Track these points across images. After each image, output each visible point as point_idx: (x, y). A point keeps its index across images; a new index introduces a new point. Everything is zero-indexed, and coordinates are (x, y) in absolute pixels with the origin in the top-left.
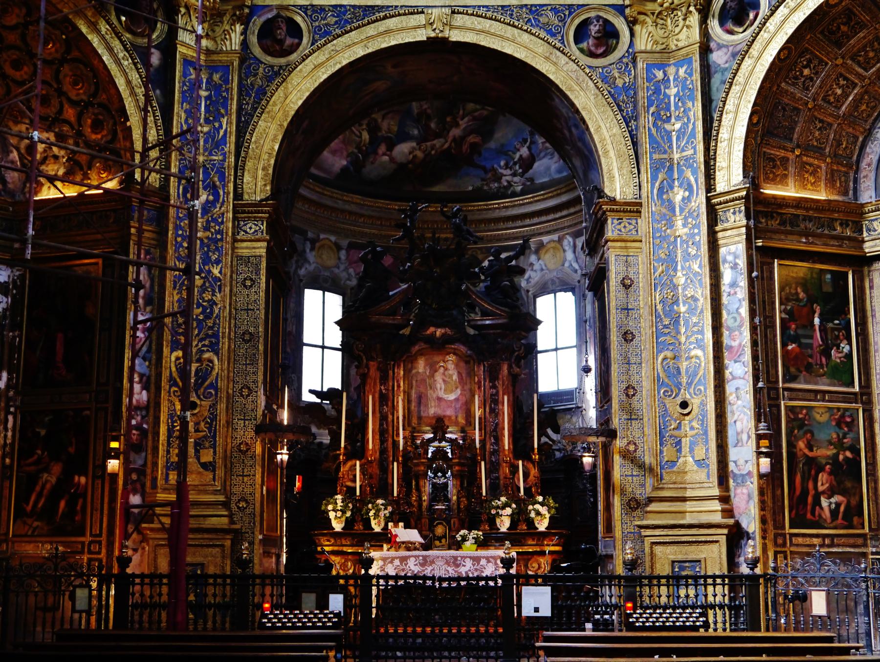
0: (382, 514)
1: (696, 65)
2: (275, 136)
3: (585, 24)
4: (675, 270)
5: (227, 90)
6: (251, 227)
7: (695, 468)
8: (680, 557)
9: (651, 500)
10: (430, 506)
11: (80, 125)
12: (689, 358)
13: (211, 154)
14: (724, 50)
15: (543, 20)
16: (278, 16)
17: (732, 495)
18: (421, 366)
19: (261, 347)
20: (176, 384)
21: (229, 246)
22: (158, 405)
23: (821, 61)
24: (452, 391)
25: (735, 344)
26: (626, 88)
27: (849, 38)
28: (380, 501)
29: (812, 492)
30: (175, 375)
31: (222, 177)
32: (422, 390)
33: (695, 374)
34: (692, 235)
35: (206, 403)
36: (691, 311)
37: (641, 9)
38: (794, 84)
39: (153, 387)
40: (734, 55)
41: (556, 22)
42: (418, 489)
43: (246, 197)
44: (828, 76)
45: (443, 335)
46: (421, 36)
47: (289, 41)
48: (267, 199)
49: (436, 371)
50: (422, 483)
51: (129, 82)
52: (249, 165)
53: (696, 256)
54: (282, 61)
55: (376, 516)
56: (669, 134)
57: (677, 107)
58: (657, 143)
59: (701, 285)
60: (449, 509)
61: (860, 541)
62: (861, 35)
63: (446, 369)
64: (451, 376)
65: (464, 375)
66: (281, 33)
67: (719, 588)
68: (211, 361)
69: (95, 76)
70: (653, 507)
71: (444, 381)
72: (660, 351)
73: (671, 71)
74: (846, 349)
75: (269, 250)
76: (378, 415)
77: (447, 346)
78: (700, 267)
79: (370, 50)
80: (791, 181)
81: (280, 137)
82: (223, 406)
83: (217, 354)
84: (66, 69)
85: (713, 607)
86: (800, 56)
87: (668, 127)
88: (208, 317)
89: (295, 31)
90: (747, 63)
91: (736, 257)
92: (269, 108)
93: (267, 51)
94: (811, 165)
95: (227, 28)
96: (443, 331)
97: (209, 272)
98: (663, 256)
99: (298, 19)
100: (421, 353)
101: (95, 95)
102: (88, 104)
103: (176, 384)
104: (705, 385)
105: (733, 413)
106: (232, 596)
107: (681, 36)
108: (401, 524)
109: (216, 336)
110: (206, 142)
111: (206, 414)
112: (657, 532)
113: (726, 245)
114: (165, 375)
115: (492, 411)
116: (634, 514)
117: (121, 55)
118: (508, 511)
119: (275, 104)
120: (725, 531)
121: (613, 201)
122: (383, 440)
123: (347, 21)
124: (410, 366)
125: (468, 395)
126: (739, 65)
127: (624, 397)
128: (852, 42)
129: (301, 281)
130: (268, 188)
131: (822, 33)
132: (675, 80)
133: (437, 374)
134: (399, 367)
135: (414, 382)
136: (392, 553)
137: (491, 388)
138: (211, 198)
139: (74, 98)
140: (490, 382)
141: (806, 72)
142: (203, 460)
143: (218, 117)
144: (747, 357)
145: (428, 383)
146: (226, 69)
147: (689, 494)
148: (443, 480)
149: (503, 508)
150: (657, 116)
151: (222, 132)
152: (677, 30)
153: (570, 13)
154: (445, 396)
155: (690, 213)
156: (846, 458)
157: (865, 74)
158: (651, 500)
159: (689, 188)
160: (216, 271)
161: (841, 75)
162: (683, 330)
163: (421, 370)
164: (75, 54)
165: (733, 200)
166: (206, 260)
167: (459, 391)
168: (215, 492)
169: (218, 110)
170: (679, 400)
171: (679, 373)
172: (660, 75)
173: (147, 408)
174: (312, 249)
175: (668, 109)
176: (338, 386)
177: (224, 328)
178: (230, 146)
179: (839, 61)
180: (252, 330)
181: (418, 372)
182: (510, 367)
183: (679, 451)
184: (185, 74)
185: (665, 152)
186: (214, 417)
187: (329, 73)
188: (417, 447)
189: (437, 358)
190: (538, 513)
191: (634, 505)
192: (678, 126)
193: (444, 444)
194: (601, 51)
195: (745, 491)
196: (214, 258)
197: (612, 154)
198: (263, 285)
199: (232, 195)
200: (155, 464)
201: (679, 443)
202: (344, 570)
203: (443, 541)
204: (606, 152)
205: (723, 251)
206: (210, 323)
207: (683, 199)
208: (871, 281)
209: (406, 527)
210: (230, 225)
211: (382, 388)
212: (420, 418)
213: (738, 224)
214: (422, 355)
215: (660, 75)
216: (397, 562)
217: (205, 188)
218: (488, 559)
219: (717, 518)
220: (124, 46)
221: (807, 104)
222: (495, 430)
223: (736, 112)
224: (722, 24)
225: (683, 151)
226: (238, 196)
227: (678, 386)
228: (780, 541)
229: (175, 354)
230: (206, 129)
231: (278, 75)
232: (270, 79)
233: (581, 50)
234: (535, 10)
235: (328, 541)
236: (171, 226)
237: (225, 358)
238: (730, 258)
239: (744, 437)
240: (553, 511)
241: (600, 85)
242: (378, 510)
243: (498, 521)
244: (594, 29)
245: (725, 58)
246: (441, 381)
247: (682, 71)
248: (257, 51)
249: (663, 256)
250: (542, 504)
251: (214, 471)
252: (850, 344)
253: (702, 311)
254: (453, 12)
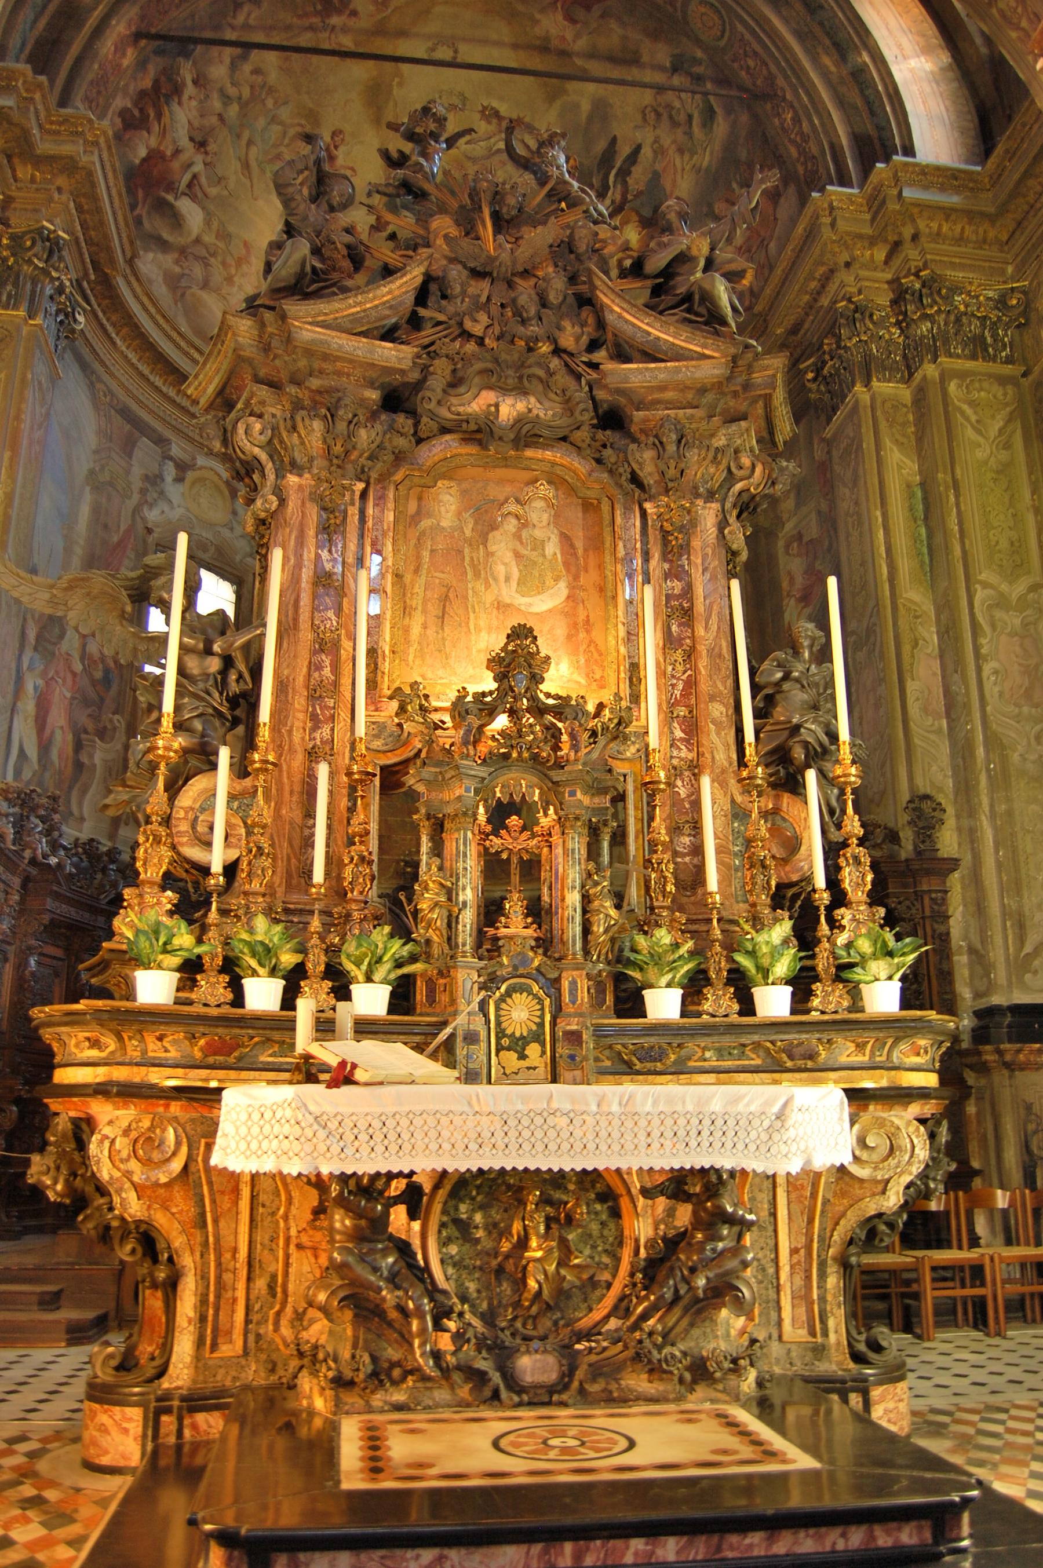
24: (541, 589)
45: (520, 421)
49: (494, 527)
63: (524, 524)
64: (539, 545)
65: (579, 545)
71: (517, 555)
77: (529, 453)
96: (521, 406)
100: (447, 471)
124: (412, 507)
129: (149, 531)
133: (495, 536)
134: (381, 498)
135: (426, 554)
137: (667, 576)
140: (664, 557)
163: (447, 521)
174: (180, 480)
181: (437, 528)
189: (496, 492)
202: (147, 1162)
203: (533, 1050)
211: (325, 554)
235: (95, 1044)
246: (509, 556)
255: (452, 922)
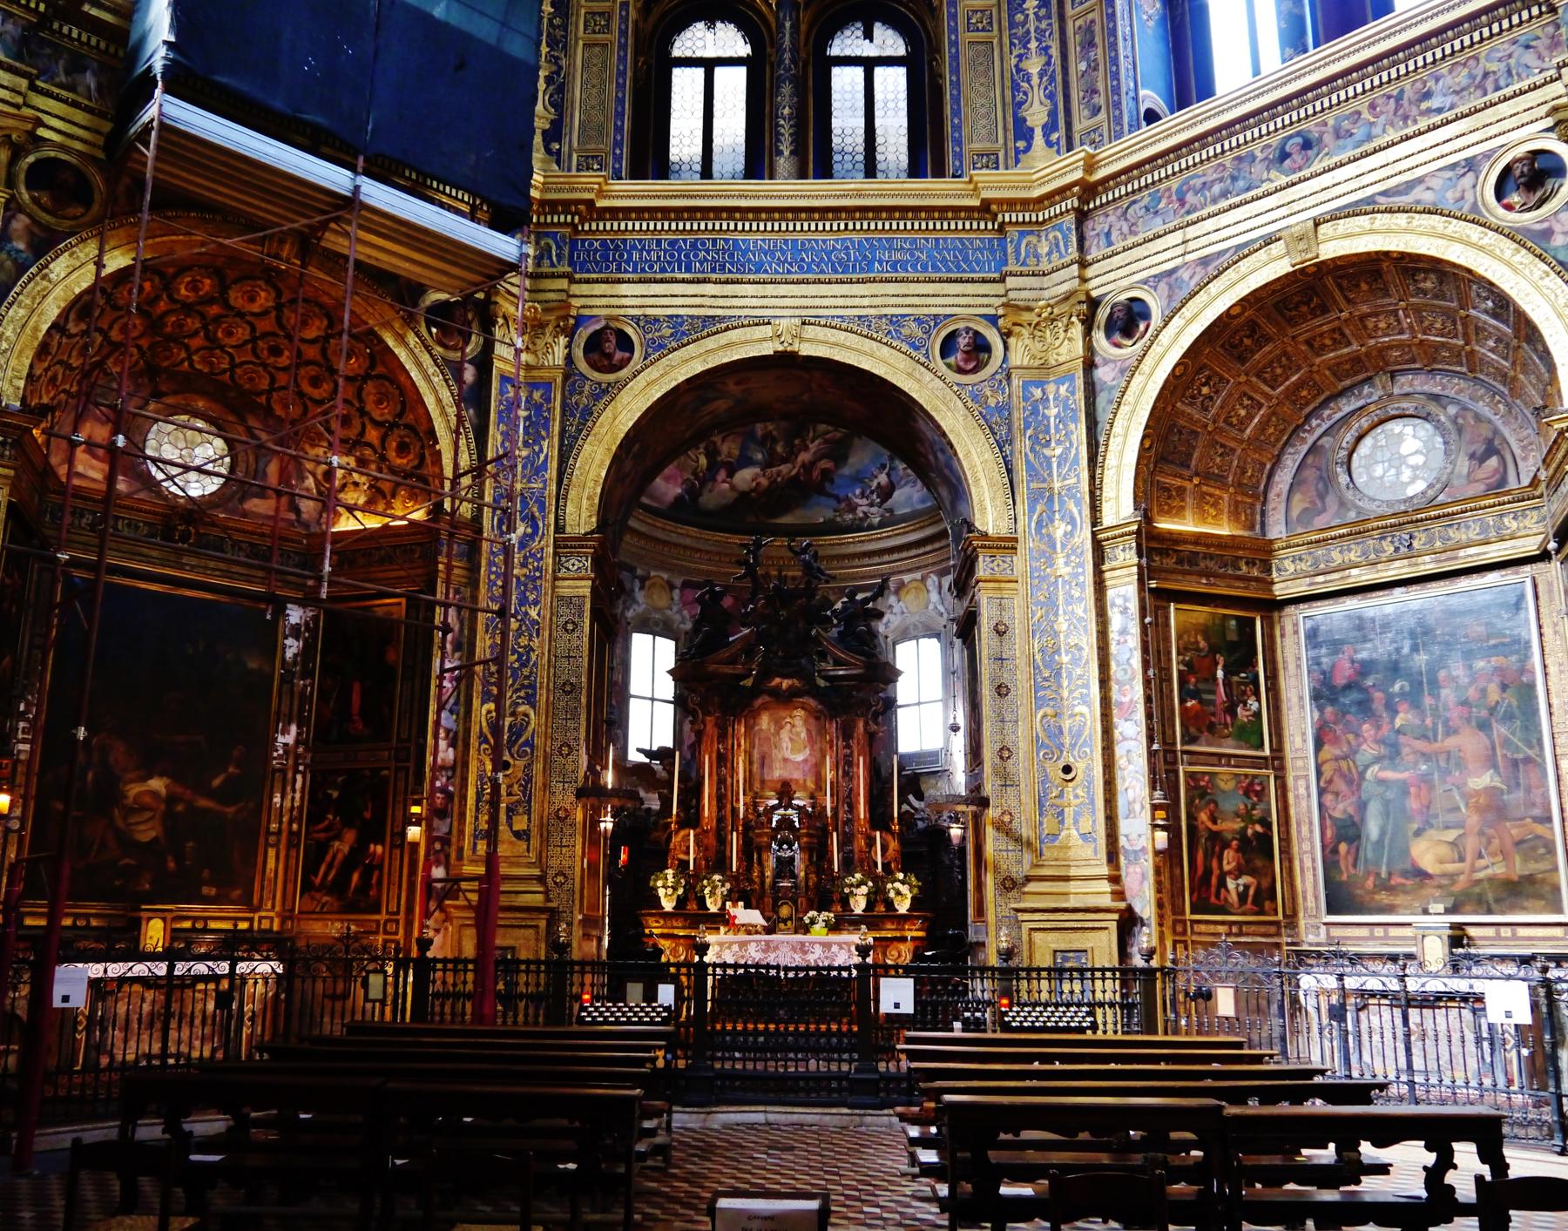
0: (718, 891)
1: (1080, 382)
2: (602, 462)
3: (951, 338)
4: (1056, 614)
5: (549, 410)
6: (573, 564)
7: (1080, 842)
8: (1063, 947)
9: (1028, 879)
10: (774, 883)
11: (384, 448)
12: (1073, 716)
13: (529, 481)
14: (1111, 365)
15: (905, 331)
16: (607, 327)
17: (1123, 873)
18: (765, 721)
19: (584, 700)
20: (486, 741)
21: (549, 585)
22: (465, 765)
23: (1222, 379)
24: (799, 751)
25: (1125, 700)
26: (999, 408)
27: (1253, 353)
28: (717, 877)
29: (1216, 872)
30: (486, 730)
31: (542, 507)
32: (765, 749)
33: (1080, 733)
34: (1076, 575)
35: (520, 763)
36: (1075, 662)
37: (1016, 319)
38: (1191, 404)
39: (460, 743)
40: (1122, 371)
41: (920, 334)
42: (760, 863)
43: (568, 529)
44: (1230, 395)
45: (790, 687)
46: (768, 349)
47: (619, 355)
48: (592, 532)
50: (764, 856)
51: (439, 401)
52: (572, 494)
53: (1080, 599)
54: (611, 377)
55: (712, 893)
56: (1048, 459)
57: (1057, 430)
58: (1035, 469)
59: (1086, 631)
60: (796, 886)
61: (1273, 929)
62: (1267, 349)
64: (798, 734)
66: (610, 346)
67: (1109, 983)
68: (527, 715)
69: (401, 394)
70: (1032, 887)
72: (1039, 708)
73: (1051, 388)
74: (1255, 706)
75: (594, 589)
76: (715, 778)
78: (1085, 611)
79: (710, 366)
80: (1188, 513)
81: (608, 463)
82: (540, 766)
83: (534, 707)
84: (370, 387)
85: (1101, 1005)
86: (1198, 373)
87: (1047, 452)
88: (524, 665)
89: (625, 343)
90: (1138, 380)
91: (1126, 600)
92: (596, 429)
93: (595, 366)
94: (1211, 495)
95: (550, 340)
97: (526, 613)
98: (1042, 599)
99: (630, 331)
100: (765, 707)
101: (400, 415)
102: (393, 426)
103: (486, 741)
104: (1091, 746)
105: (1124, 779)
106: (547, 985)
107: (1061, 350)
108: (741, 904)
109: (532, 686)
110: (524, 467)
111: (520, 775)
112: (1037, 916)
113: (1115, 586)
114: (475, 730)
115: (846, 774)
116: (1010, 895)
117: (430, 371)
118: (864, 889)
119: (602, 426)
120: (1116, 916)
121: (985, 536)
122: (720, 807)
123: (683, 333)
125: (818, 755)
126: (1129, 382)
127: (997, 760)
128: (1257, 357)
130: (594, 519)
131: (1222, 346)
132: (1055, 399)
136: (731, 937)
138: (529, 530)
139: (378, 418)
141: (1205, 390)
142: (515, 828)
143: (538, 439)
144: (1140, 714)
145: (772, 741)
146: (547, 386)
147: (1073, 872)
148: (789, 854)
149: (858, 886)
150: (1035, 439)
151: (542, 457)
152: (1057, 343)
153: (936, 324)
154: (792, 757)
155: (1074, 551)
156: (1256, 833)
157: (1272, 392)
158: (1028, 879)
159: (1072, 522)
160: (533, 613)
161: (1245, 394)
162: (1065, 683)
164: (380, 369)
165: (1122, 535)
166: (523, 601)
167: (808, 751)
168: (529, 865)
169: (538, 432)
170: (1061, 764)
171: (1061, 732)
172: (1038, 393)
173: (453, 768)
175: (1047, 432)
176: (670, 744)
177: (542, 677)
178: (552, 472)
179: (1243, 378)
180: (573, 680)
182: (866, 724)
183: (1062, 822)
184: (502, 393)
185: (1044, 481)
186: (529, 779)
187: (664, 391)
188: (759, 815)
189: (782, 713)
190: (898, 893)
191: (1009, 885)
192: (1058, 451)
193: (790, 811)
194: (971, 366)
195: (1138, 870)
196: (531, 597)
197: (983, 482)
198: (587, 629)
199: (552, 528)
200: (461, 832)
201: (1061, 813)
204: (977, 480)
205: (1110, 594)
206: (526, 672)
207: (1065, 534)
208: (1282, 628)
209: (746, 907)
210: (550, 561)
212: (763, 782)
213: (1129, 562)
214: (766, 709)
215: (1038, 393)
216: (735, 948)
217: (522, 520)
218: (840, 945)
219: (1106, 901)
220: (435, 361)
221: (1206, 426)
222: (849, 796)
223: (1126, 436)
224: (1108, 335)
225: (1065, 479)
226: (559, 528)
227: (1060, 747)
228: (1179, 928)
229: (486, 707)
230: (524, 453)
231: (605, 393)
232: (597, 398)
233: (949, 366)
234: (896, 321)
236: (484, 562)
237: (543, 711)
238: (1119, 601)
239: (1137, 807)
240: (915, 891)
241: (970, 404)
242: (715, 888)
243: (852, 901)
244: (963, 342)
245: (1112, 375)
247: (1063, 389)
248: (582, 366)
249: (1042, 599)
250: (903, 883)
251: (528, 840)
252: (1259, 700)
253: (1087, 662)
254: (804, 323)
255: (763, 883)
